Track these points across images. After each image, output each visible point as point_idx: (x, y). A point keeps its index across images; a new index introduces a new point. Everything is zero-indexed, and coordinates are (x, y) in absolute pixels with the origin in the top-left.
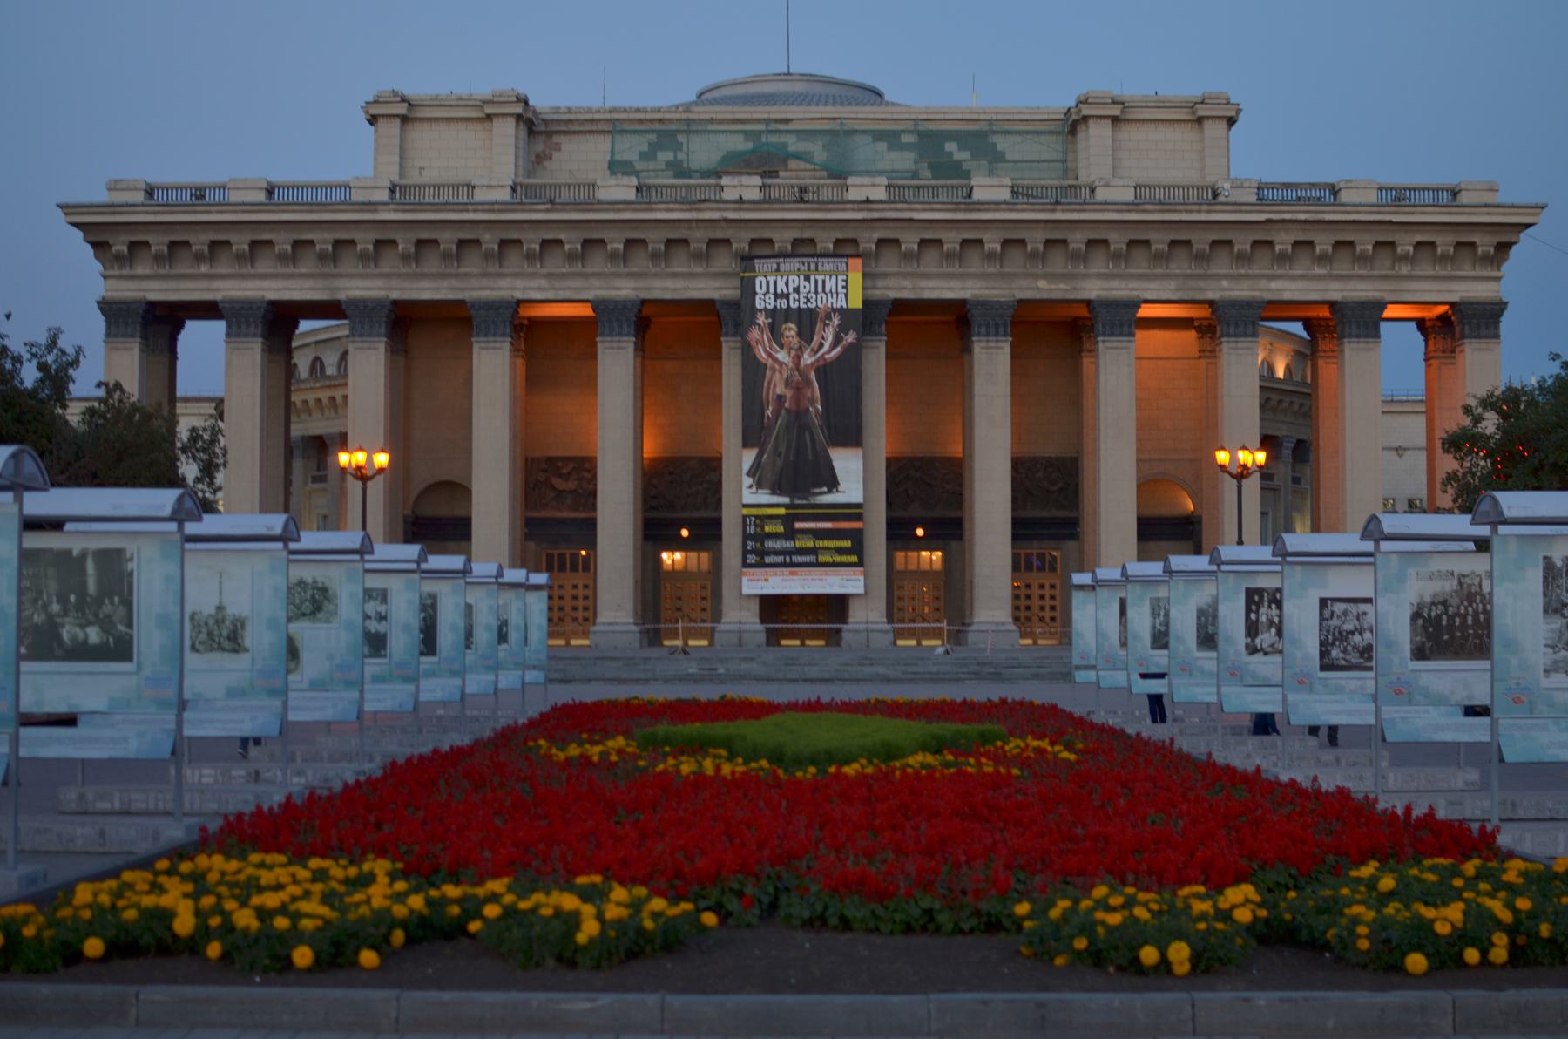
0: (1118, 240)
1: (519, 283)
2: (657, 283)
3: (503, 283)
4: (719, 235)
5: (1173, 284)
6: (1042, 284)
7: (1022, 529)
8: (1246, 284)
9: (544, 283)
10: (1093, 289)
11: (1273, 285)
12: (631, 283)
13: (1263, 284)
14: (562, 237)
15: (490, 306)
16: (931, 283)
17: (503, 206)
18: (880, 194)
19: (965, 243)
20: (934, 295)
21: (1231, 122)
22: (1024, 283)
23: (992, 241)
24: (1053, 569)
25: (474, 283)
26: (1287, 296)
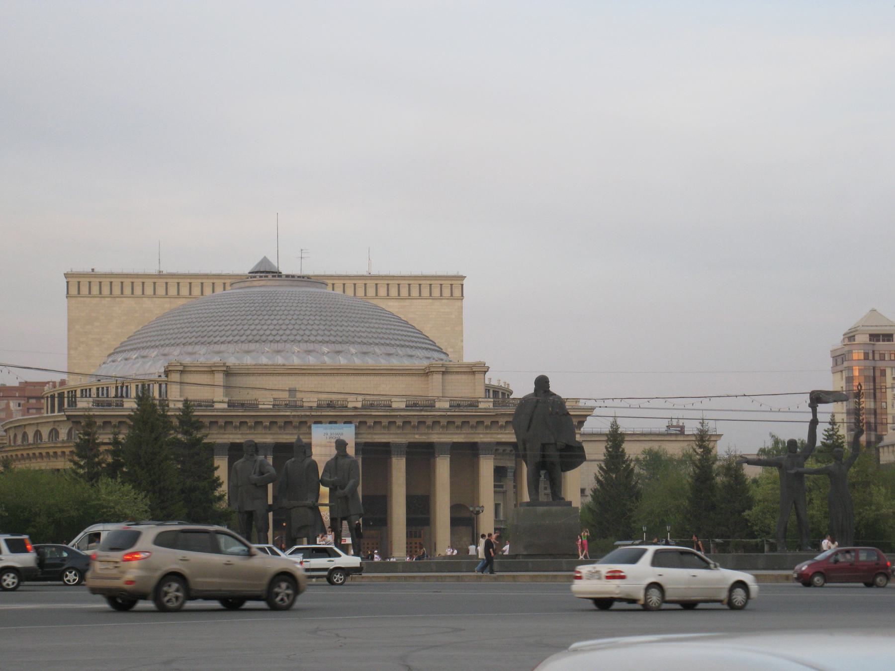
0: (444, 422)
1: (231, 436)
2: (281, 436)
3: (226, 436)
4: (304, 420)
5: (463, 436)
6: (417, 436)
7: (410, 522)
8: (489, 436)
9: (240, 436)
10: (436, 437)
11: (499, 436)
12: (272, 437)
13: (495, 436)
14: (247, 420)
15: (222, 446)
16: (377, 436)
17: (223, 410)
18: (359, 405)
19: (390, 422)
20: (379, 441)
21: (485, 372)
22: (410, 436)
23: (399, 422)
24: (420, 536)
25: (215, 436)
26: (503, 440)
